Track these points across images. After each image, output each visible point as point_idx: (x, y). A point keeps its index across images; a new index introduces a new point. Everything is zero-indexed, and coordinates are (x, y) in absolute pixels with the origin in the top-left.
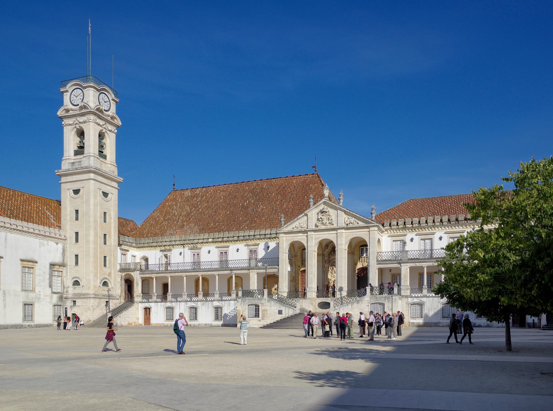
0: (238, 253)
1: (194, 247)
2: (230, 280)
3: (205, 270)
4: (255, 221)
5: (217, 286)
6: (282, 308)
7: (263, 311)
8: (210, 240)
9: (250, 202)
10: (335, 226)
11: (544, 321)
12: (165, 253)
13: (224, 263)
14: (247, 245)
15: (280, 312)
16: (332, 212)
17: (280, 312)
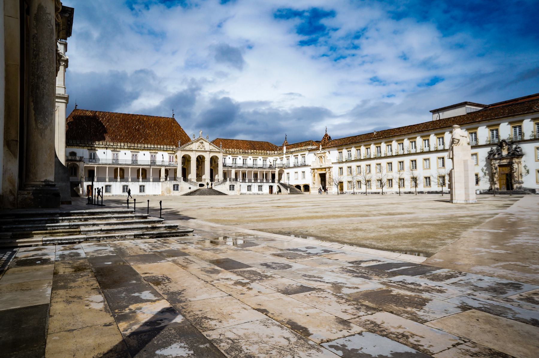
0: (144, 157)
1: (114, 150)
2: (138, 170)
3: (121, 165)
4: (148, 139)
5: (151, 175)
6: (191, 186)
7: (181, 187)
8: (126, 147)
9: (139, 127)
10: (206, 150)
11: (289, 192)
12: (91, 151)
13: (135, 162)
14: (150, 153)
15: (190, 188)
16: (204, 142)
17: (190, 188)
